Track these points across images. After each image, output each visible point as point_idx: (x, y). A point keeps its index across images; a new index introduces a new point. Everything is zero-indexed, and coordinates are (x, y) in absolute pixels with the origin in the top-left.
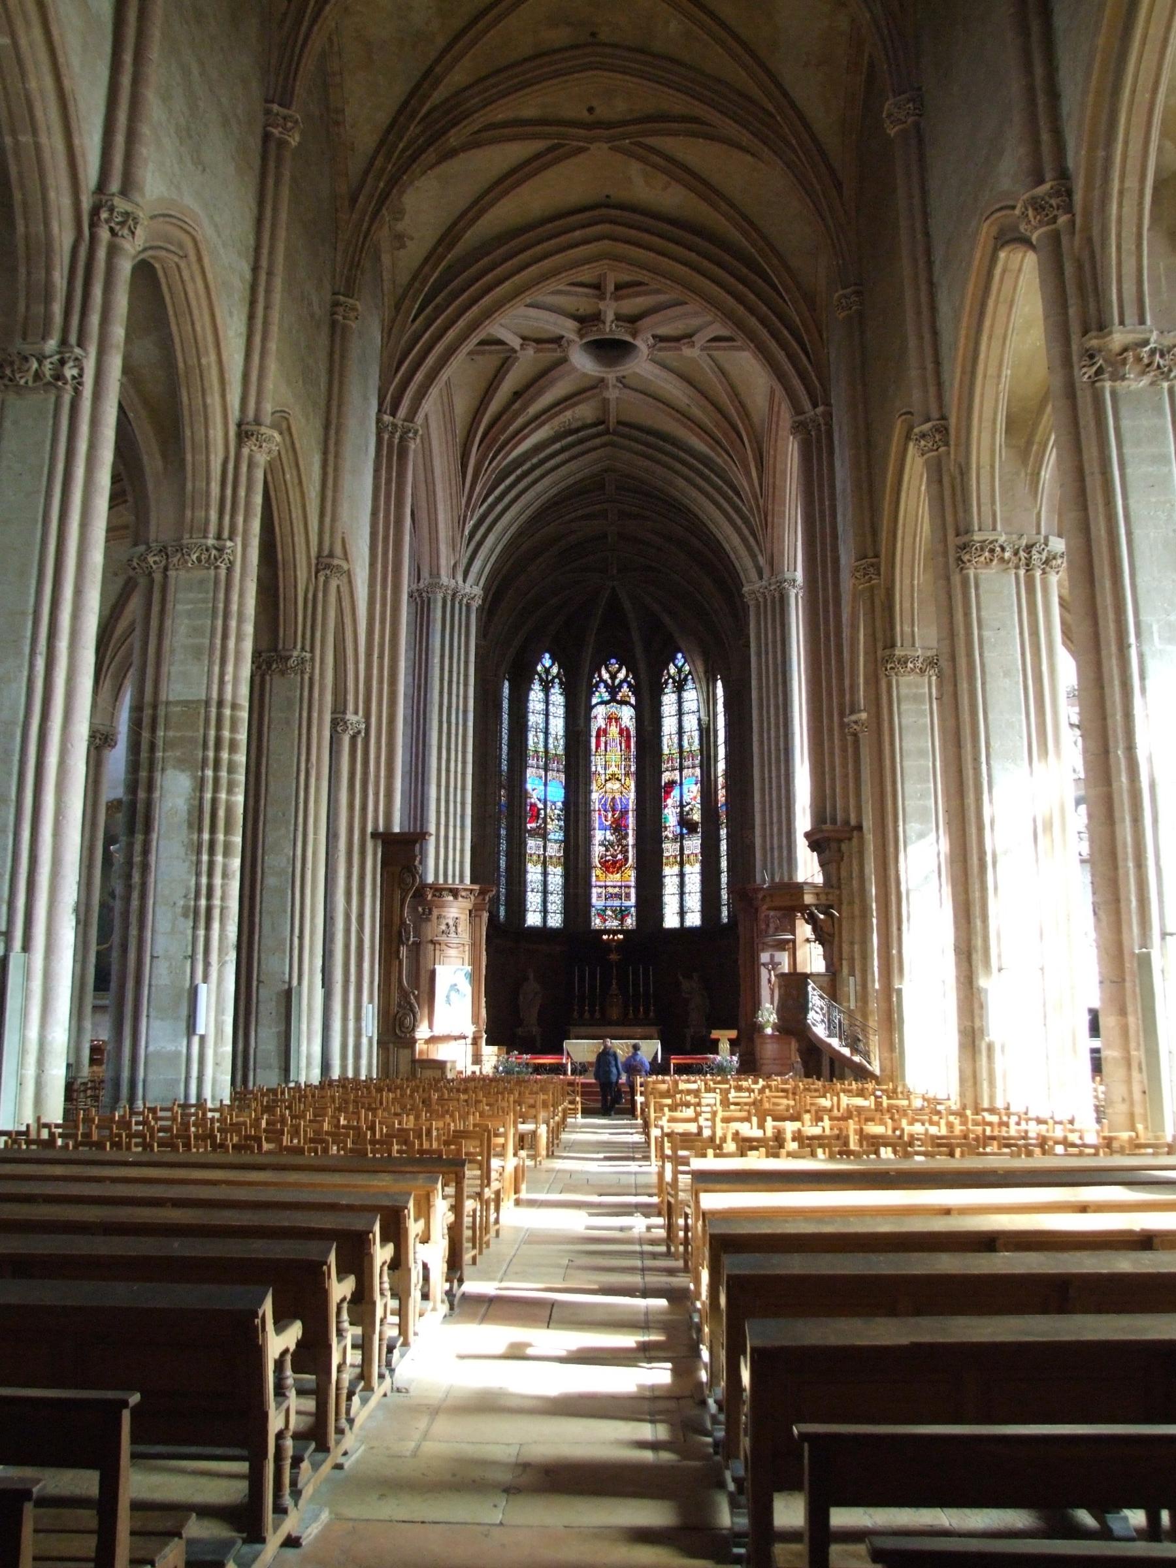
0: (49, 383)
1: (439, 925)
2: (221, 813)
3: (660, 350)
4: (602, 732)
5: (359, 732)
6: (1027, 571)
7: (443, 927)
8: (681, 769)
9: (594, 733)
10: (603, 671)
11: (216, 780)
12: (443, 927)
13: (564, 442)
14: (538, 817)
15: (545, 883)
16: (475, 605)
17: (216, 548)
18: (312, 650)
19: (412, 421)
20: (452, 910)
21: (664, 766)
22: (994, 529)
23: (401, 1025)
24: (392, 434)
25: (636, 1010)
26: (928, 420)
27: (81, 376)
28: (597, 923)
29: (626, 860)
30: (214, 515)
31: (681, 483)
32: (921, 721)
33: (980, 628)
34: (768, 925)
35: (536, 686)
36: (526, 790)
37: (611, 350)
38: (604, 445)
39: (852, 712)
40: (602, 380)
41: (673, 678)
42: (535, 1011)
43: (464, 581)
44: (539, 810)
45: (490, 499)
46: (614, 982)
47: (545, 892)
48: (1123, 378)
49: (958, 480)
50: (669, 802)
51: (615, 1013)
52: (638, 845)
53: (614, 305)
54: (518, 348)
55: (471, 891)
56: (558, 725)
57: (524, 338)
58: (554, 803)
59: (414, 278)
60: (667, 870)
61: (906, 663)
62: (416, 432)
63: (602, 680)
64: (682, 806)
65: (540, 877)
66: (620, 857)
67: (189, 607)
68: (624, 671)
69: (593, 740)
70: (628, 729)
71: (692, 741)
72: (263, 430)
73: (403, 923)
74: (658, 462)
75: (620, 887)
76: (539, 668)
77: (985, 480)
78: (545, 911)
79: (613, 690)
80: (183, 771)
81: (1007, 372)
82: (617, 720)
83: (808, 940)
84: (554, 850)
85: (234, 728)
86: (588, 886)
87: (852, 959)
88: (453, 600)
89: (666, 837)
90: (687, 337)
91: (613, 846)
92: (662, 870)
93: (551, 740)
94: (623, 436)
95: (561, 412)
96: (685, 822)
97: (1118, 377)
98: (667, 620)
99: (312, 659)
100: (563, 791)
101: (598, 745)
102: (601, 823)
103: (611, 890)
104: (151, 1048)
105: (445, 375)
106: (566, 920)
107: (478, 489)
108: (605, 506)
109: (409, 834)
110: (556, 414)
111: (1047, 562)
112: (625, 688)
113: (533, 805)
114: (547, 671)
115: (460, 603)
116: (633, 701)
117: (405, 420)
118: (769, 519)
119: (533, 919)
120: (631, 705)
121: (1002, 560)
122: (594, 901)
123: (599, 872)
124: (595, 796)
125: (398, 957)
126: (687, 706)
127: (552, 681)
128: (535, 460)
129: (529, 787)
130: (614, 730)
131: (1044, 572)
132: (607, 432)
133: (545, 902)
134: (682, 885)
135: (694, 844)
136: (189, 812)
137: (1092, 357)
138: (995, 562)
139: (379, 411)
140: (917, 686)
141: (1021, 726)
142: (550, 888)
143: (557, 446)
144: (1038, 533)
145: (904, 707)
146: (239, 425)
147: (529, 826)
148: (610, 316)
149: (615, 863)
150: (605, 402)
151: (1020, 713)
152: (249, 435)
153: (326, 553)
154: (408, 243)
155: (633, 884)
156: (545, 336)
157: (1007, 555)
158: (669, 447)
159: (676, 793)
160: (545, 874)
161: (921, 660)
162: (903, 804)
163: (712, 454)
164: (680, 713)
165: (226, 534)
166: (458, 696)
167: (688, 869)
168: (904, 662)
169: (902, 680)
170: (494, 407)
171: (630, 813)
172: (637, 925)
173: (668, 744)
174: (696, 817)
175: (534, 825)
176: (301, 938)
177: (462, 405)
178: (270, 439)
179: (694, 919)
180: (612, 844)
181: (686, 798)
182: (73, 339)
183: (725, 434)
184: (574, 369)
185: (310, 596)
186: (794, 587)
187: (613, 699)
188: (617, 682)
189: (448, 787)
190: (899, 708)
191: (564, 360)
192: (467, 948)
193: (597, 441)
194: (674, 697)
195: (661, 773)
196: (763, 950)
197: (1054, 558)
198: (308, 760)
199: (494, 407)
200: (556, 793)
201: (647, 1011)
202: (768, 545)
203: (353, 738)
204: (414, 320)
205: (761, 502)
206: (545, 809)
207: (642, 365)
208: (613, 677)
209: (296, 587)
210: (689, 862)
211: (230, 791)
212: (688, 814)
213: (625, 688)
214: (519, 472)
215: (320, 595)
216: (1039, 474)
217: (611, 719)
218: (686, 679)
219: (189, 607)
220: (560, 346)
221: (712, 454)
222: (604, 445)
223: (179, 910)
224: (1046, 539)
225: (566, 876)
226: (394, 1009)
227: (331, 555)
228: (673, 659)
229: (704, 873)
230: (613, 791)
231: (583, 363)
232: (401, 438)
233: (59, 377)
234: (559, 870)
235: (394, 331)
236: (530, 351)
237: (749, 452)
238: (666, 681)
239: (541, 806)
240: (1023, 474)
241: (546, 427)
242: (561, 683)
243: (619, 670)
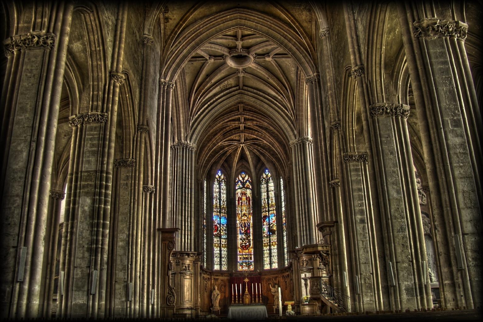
0: (42, 45)
1: (182, 267)
2: (102, 212)
3: (258, 58)
4: (240, 199)
5: (153, 191)
6: (396, 117)
7: (184, 268)
8: (269, 211)
9: (237, 199)
10: (240, 177)
11: (100, 200)
12: (184, 268)
13: (225, 93)
14: (217, 230)
15: (220, 254)
16: (194, 150)
17: (100, 115)
18: (136, 159)
19: (171, 81)
20: (188, 261)
21: (263, 210)
22: (383, 102)
23: (169, 300)
24: (164, 86)
25: (255, 300)
26: (356, 65)
27: (54, 43)
28: (240, 268)
29: (250, 245)
30: (100, 103)
31: (266, 106)
32: (359, 178)
33: (380, 137)
34: (303, 264)
35: (216, 183)
36: (213, 220)
37: (240, 59)
38: (239, 93)
39: (332, 180)
40: (238, 70)
41: (265, 179)
42: (218, 301)
43: (190, 142)
44: (218, 227)
45: (199, 113)
47: (221, 257)
48: (429, 36)
49: (369, 86)
50: (265, 223)
52: (254, 239)
53: (241, 43)
54: (208, 59)
55: (194, 254)
56: (224, 197)
57: (210, 55)
58: (223, 225)
59: (172, 33)
60: (265, 248)
61: (352, 157)
62: (173, 85)
63: (239, 180)
64: (269, 224)
65: (219, 252)
66: (247, 244)
67: (90, 137)
68: (247, 177)
69: (237, 202)
70: (249, 197)
71: (273, 201)
72: (119, 74)
73: (169, 262)
74: (258, 99)
75: (248, 255)
76: (217, 176)
77: (378, 85)
78: (221, 264)
79: (243, 184)
80: (88, 197)
81: (384, 47)
82: (245, 194)
83: (318, 268)
84: (223, 242)
85: (107, 181)
86: (236, 255)
87: (336, 271)
88: (186, 149)
89: (264, 236)
90: (267, 54)
91: (245, 240)
92: (262, 248)
93: (222, 202)
94: (245, 90)
95: (223, 82)
96: (271, 231)
97: (427, 35)
98: (262, 158)
99: (136, 162)
100: (226, 220)
101: (239, 204)
102: (240, 232)
103: (244, 256)
104: (73, 303)
105: (183, 66)
107: (194, 109)
108: (239, 116)
109: (171, 229)
110: (222, 83)
111: (403, 113)
112: (248, 183)
113: (216, 226)
114: (220, 177)
115: (189, 150)
116: (251, 187)
117: (169, 81)
118: (298, 117)
119: (216, 267)
120: (250, 189)
121: (387, 113)
122: (239, 260)
123: (240, 250)
124: (238, 222)
125: (168, 275)
126: (270, 188)
127: (222, 181)
128: (214, 99)
129: (214, 219)
130: (244, 198)
131: (402, 117)
132: (239, 89)
133: (221, 261)
134: (270, 254)
135: (274, 238)
136: (90, 212)
137: (417, 29)
138: (384, 114)
139: (160, 78)
140: (357, 166)
141: (398, 172)
142: (223, 256)
143: (222, 94)
144: (399, 103)
145: (352, 173)
146: (110, 72)
147: (214, 233)
148: (240, 47)
149: (246, 246)
150: (238, 77)
151: (397, 167)
152: (113, 76)
153: (141, 123)
154: (170, 21)
155: (253, 254)
156: (218, 54)
157: (388, 111)
158: (261, 94)
159: (267, 220)
160: (220, 251)
161: (357, 156)
162: (354, 208)
163: (277, 96)
164: (268, 191)
165: (105, 111)
166: (188, 183)
167: (272, 247)
168: (351, 157)
169: (351, 164)
170: (199, 80)
171: (251, 228)
173: (264, 202)
174: (275, 228)
175: (216, 233)
176: (131, 265)
177: (188, 80)
178: (122, 77)
179: (275, 266)
180: (244, 239)
181: (271, 222)
182: (51, 31)
183: (281, 88)
184: (228, 66)
185: (135, 139)
186: (308, 141)
187: (244, 187)
188: (245, 181)
189: (185, 216)
190: (350, 174)
191: (225, 63)
192: (193, 275)
193: (236, 92)
194: (265, 185)
195: (261, 213)
196: (302, 273)
197: (405, 111)
198: (134, 199)
199: (199, 80)
200: (224, 221)
201: (259, 300)
202: (298, 127)
203: (151, 194)
204: (172, 47)
205: (295, 112)
206: (220, 227)
207: (251, 64)
208: (243, 179)
209: (130, 135)
210: (273, 245)
211: (105, 204)
212: (272, 227)
213: (248, 183)
214: (209, 103)
215: (139, 139)
216: (397, 82)
217: (244, 194)
218: (269, 179)
219: (90, 137)
220: (223, 58)
221: (277, 96)
222: (239, 93)
223: (85, 249)
224: (402, 105)
225: (228, 251)
226: (167, 294)
227: (143, 125)
228: (265, 172)
229: (278, 249)
230: (244, 220)
231: (231, 63)
232: (167, 87)
233: (45, 43)
234: (226, 249)
235: (165, 50)
236: (212, 60)
237: (290, 94)
238: (262, 180)
239: (218, 226)
240: (392, 83)
241: (218, 87)
242: (225, 181)
243: (245, 176)
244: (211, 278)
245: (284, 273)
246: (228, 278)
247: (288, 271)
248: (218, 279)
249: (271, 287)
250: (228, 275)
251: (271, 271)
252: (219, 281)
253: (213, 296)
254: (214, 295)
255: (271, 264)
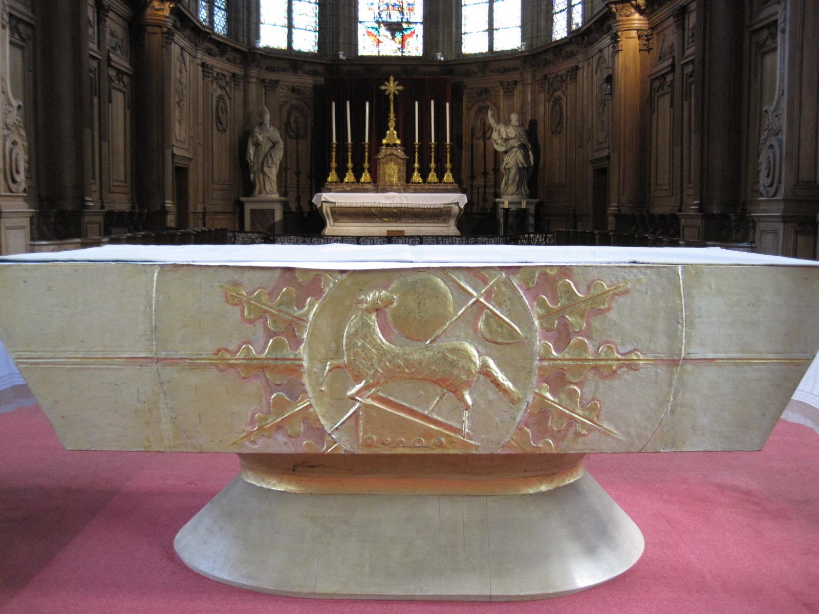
42: (273, 172)
46: (392, 124)
51: (392, 171)
106: (321, 43)
172: (425, 50)
244: (246, 77)
245: (547, 63)
246: (321, 80)
247: (572, 55)
248: (277, 82)
249: (491, 121)
250: (320, 69)
251: (492, 61)
252: (282, 92)
253: (251, 150)
254: (257, 145)
255: (491, 30)
